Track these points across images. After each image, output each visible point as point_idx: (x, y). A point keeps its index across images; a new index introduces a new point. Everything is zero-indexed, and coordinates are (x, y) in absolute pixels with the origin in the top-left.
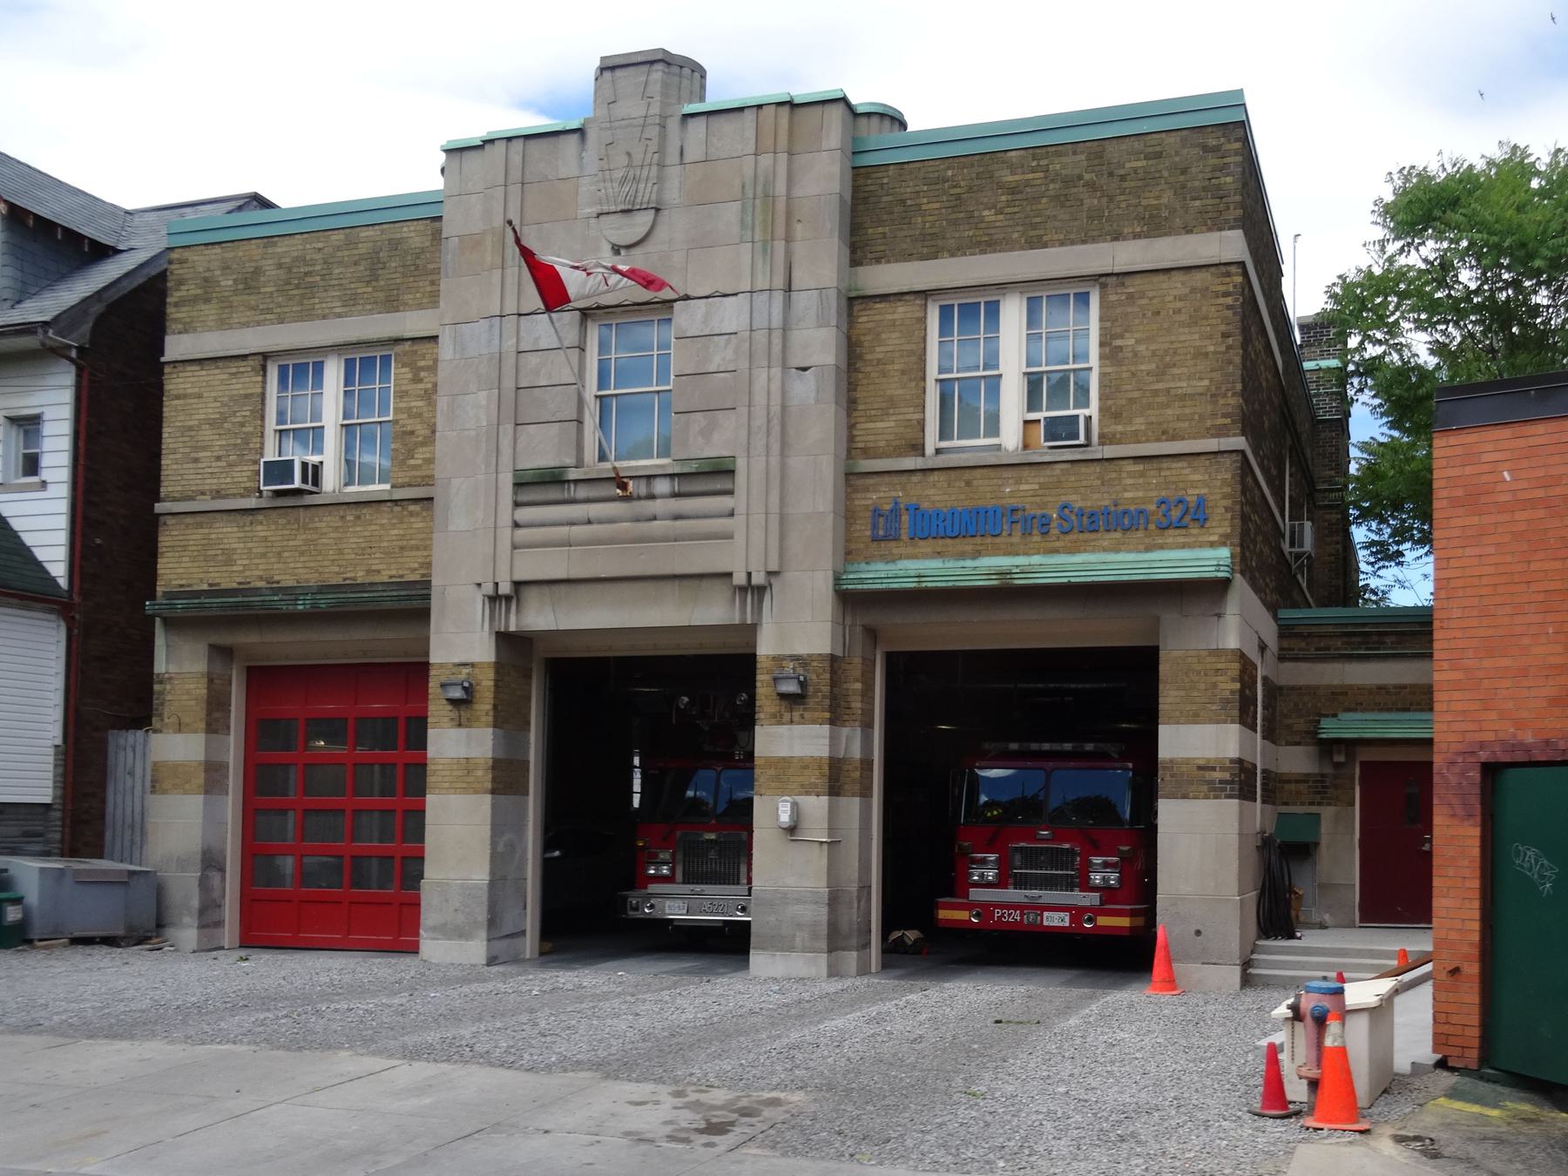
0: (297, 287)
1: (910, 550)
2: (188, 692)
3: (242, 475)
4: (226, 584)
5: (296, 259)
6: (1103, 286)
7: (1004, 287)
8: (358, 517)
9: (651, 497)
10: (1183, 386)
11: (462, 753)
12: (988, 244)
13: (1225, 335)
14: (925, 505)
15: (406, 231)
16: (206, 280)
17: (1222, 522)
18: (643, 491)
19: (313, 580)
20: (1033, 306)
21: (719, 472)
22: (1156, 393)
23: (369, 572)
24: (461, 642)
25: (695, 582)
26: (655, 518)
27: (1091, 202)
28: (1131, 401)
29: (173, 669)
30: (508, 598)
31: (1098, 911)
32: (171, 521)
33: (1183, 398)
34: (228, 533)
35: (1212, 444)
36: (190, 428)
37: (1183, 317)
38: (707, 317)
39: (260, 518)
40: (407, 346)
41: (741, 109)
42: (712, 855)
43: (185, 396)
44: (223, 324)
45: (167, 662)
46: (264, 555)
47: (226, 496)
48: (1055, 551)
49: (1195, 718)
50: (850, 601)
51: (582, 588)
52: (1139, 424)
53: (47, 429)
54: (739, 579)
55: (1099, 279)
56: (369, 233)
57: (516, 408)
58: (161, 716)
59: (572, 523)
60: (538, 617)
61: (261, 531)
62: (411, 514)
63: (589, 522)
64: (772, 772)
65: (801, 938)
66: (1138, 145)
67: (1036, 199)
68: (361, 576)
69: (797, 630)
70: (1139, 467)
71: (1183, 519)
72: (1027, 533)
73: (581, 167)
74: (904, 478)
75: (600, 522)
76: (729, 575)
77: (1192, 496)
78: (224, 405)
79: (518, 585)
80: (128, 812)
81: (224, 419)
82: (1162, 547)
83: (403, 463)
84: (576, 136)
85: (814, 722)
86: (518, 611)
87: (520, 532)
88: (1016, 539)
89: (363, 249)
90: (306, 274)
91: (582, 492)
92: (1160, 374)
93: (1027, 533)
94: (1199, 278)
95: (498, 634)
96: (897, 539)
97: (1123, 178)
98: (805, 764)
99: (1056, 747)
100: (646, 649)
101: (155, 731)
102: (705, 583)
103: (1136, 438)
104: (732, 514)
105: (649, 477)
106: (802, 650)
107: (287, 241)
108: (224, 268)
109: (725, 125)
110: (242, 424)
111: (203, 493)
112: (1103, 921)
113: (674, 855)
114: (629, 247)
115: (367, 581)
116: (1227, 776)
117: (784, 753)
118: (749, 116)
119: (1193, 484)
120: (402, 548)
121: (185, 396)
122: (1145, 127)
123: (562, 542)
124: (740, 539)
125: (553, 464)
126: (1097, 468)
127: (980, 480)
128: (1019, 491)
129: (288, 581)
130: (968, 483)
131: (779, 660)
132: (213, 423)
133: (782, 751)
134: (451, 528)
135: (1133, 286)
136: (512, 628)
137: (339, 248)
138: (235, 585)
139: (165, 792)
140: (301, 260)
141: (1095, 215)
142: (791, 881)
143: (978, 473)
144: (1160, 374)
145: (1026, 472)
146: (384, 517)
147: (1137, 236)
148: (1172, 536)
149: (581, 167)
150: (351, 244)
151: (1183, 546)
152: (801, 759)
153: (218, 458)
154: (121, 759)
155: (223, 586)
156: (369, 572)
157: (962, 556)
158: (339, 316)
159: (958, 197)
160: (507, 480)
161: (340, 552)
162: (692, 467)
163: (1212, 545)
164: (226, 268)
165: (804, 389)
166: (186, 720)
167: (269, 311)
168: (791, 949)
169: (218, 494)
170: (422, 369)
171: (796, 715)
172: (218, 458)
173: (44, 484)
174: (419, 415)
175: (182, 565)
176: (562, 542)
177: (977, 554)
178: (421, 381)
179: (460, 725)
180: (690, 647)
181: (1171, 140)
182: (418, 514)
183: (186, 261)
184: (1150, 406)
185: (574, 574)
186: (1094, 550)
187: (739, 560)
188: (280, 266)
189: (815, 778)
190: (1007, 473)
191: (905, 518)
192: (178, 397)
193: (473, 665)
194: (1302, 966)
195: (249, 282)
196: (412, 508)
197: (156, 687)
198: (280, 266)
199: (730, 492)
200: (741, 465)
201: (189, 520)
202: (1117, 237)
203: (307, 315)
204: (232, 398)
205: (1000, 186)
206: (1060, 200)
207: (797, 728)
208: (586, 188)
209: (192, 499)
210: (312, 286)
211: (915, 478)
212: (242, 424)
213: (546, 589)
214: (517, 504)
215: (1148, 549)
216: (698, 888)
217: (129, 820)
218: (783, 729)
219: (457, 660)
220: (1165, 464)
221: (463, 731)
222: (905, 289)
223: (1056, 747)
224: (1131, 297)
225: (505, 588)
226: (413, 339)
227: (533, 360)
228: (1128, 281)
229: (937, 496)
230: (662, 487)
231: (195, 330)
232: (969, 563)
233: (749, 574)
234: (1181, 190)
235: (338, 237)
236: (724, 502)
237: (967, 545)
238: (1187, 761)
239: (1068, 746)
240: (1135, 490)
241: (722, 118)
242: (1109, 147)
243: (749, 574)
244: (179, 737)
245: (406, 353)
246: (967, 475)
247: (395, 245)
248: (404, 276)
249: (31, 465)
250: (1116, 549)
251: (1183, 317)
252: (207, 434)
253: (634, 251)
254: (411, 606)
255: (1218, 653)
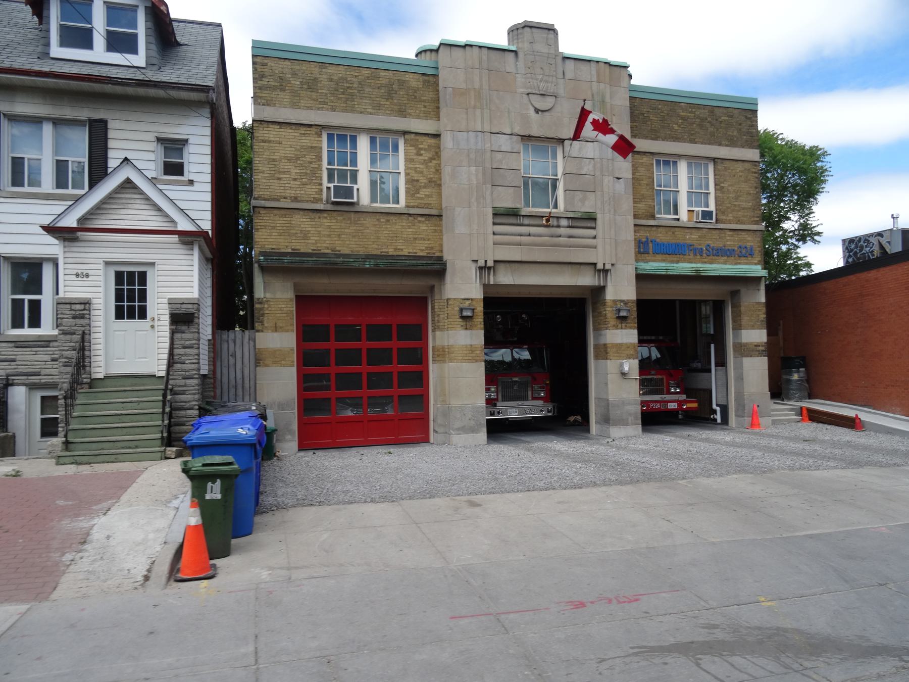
0: (343, 93)
1: (653, 258)
2: (281, 309)
3: (311, 190)
4: (303, 250)
5: (341, 78)
6: (715, 163)
7: (680, 156)
8: (388, 221)
9: (558, 226)
10: (744, 205)
11: (468, 342)
12: (676, 139)
13: (756, 188)
14: (658, 240)
15: (407, 77)
16: (281, 78)
17: (758, 257)
18: (555, 223)
19: (362, 251)
20: (373, 141)
21: (589, 219)
22: (735, 206)
23: (396, 249)
24: (464, 287)
25: (578, 266)
26: (560, 236)
27: (711, 129)
28: (728, 208)
29: (268, 295)
30: (489, 268)
31: (686, 402)
32: (263, 211)
33: (744, 209)
34: (305, 222)
35: (755, 227)
36: (274, 160)
37: (742, 179)
38: (580, 149)
39: (325, 215)
40: (413, 136)
41: (589, 61)
42: (515, 387)
43: (269, 142)
44: (294, 105)
45: (265, 292)
46: (329, 236)
47: (300, 201)
48: (705, 262)
49: (753, 327)
50: (641, 278)
51: (526, 266)
52: (730, 217)
53: (190, 149)
54: (600, 266)
55: (714, 160)
56: (390, 74)
57: (493, 176)
58: (262, 323)
59: (521, 235)
60: (505, 278)
61: (326, 222)
62: (419, 222)
63: (529, 235)
64: (615, 349)
65: (630, 419)
66: (725, 111)
67: (692, 124)
68: (391, 251)
69: (622, 290)
70: (731, 233)
71: (744, 254)
72: (695, 255)
73: (517, 69)
74: (649, 229)
75: (534, 236)
76: (595, 264)
77: (749, 245)
78: (296, 150)
79: (495, 261)
80: (239, 376)
81: (298, 159)
82: (740, 264)
83: (413, 195)
84: (513, 54)
85: (631, 328)
86: (494, 274)
87: (496, 237)
88: (692, 256)
89: (383, 81)
90: (348, 88)
91: (526, 221)
92: (737, 198)
93: (695, 255)
94: (747, 165)
95: (484, 285)
96: (648, 253)
97: (721, 122)
98: (628, 346)
99: (649, 338)
100: (524, 294)
101: (258, 331)
102: (582, 267)
103: (730, 222)
104: (595, 237)
105: (558, 218)
106: (625, 298)
107: (334, 68)
108: (292, 74)
109: (584, 67)
110: (311, 163)
111: (285, 198)
112: (689, 405)
113: (497, 388)
114: (543, 111)
115: (395, 253)
116: (763, 348)
117: (619, 341)
118: (593, 65)
119: (748, 241)
120: (415, 239)
121: (269, 142)
122: (727, 105)
123: (516, 244)
124: (600, 248)
125: (513, 206)
126: (718, 232)
127: (678, 232)
128: (691, 238)
129: (345, 251)
130: (673, 233)
131: (615, 301)
132: (289, 160)
133: (618, 341)
134: (456, 231)
135: (727, 164)
136: (492, 283)
137: (368, 78)
138: (310, 251)
139: (267, 366)
140: (344, 79)
141: (712, 134)
142: (625, 396)
143: (676, 229)
144: (737, 198)
145: (694, 231)
146: (404, 222)
147: (727, 146)
148: (743, 260)
149: (517, 69)
150: (375, 77)
151: (747, 264)
152: (626, 344)
153: (295, 179)
154: (225, 346)
155: (302, 251)
156: (396, 249)
157: (672, 262)
158: (371, 114)
159: (664, 117)
160: (490, 212)
161: (378, 238)
162: (579, 215)
163: (756, 264)
164: (294, 74)
165: (620, 187)
166: (280, 324)
167: (325, 103)
168: (627, 424)
169: (295, 199)
170: (422, 149)
171: (623, 325)
172: (295, 179)
173: (191, 182)
174: (422, 172)
175: (269, 236)
176: (516, 244)
177: (678, 262)
178: (421, 155)
179: (466, 329)
180: (556, 294)
181: (736, 112)
182: (423, 222)
183: (266, 65)
184: (733, 211)
185: (524, 259)
186: (718, 263)
187: (600, 258)
188: (331, 80)
189: (611, 351)
190: (687, 231)
191: (650, 245)
192: (264, 141)
193: (472, 300)
194: (780, 415)
195: (311, 85)
196: (420, 219)
197: (257, 306)
198: (331, 80)
199: (594, 228)
200: (599, 217)
201: (276, 212)
202: (720, 145)
203: (352, 110)
204: (302, 147)
205: (679, 116)
206: (701, 126)
207: (624, 331)
208: (520, 79)
209: (278, 200)
210: (352, 95)
211: (654, 229)
212: (311, 163)
213: (508, 265)
214: (494, 224)
215: (736, 264)
216: (520, 403)
217: (233, 382)
218: (618, 331)
219: (463, 297)
220: (740, 233)
221: (468, 332)
222: (313, 123)
223: (649, 338)
224: (726, 168)
225: (490, 264)
226: (416, 133)
227: (499, 156)
228: (725, 162)
229: (662, 237)
230: (564, 222)
231: (275, 105)
232: (675, 265)
233: (486, 261)
234: (739, 130)
235: (366, 72)
236: (592, 232)
237: (674, 258)
238: (751, 343)
239: (653, 338)
240: (731, 242)
241: (580, 62)
242: (716, 110)
243: (486, 261)
244: (275, 334)
245: (412, 140)
246: (673, 230)
247: (401, 83)
248: (408, 100)
249: (174, 169)
250: (725, 263)
251: (742, 179)
252: (285, 165)
253: (545, 113)
254: (436, 269)
255: (759, 303)
